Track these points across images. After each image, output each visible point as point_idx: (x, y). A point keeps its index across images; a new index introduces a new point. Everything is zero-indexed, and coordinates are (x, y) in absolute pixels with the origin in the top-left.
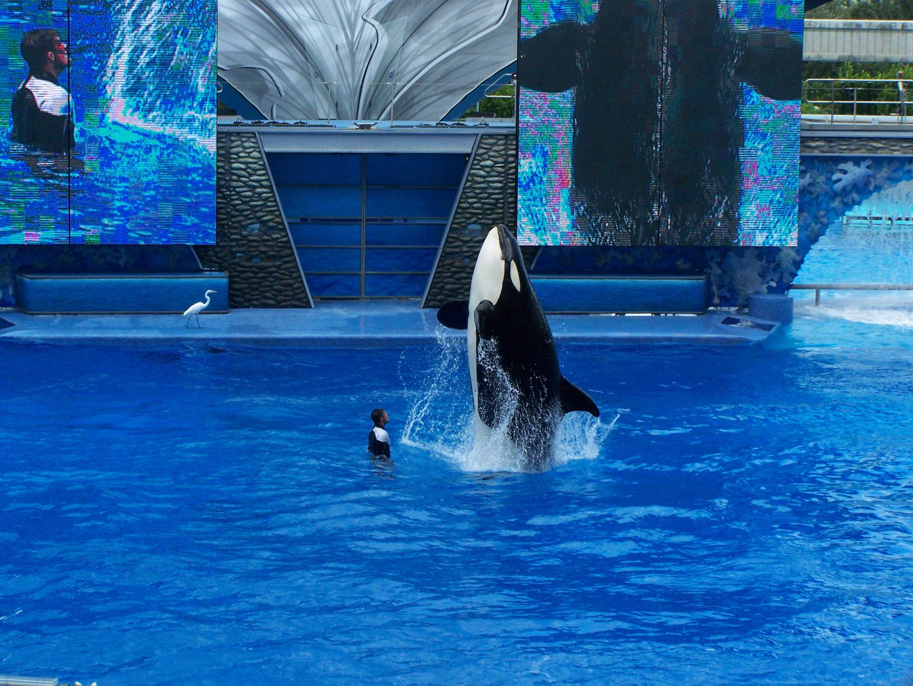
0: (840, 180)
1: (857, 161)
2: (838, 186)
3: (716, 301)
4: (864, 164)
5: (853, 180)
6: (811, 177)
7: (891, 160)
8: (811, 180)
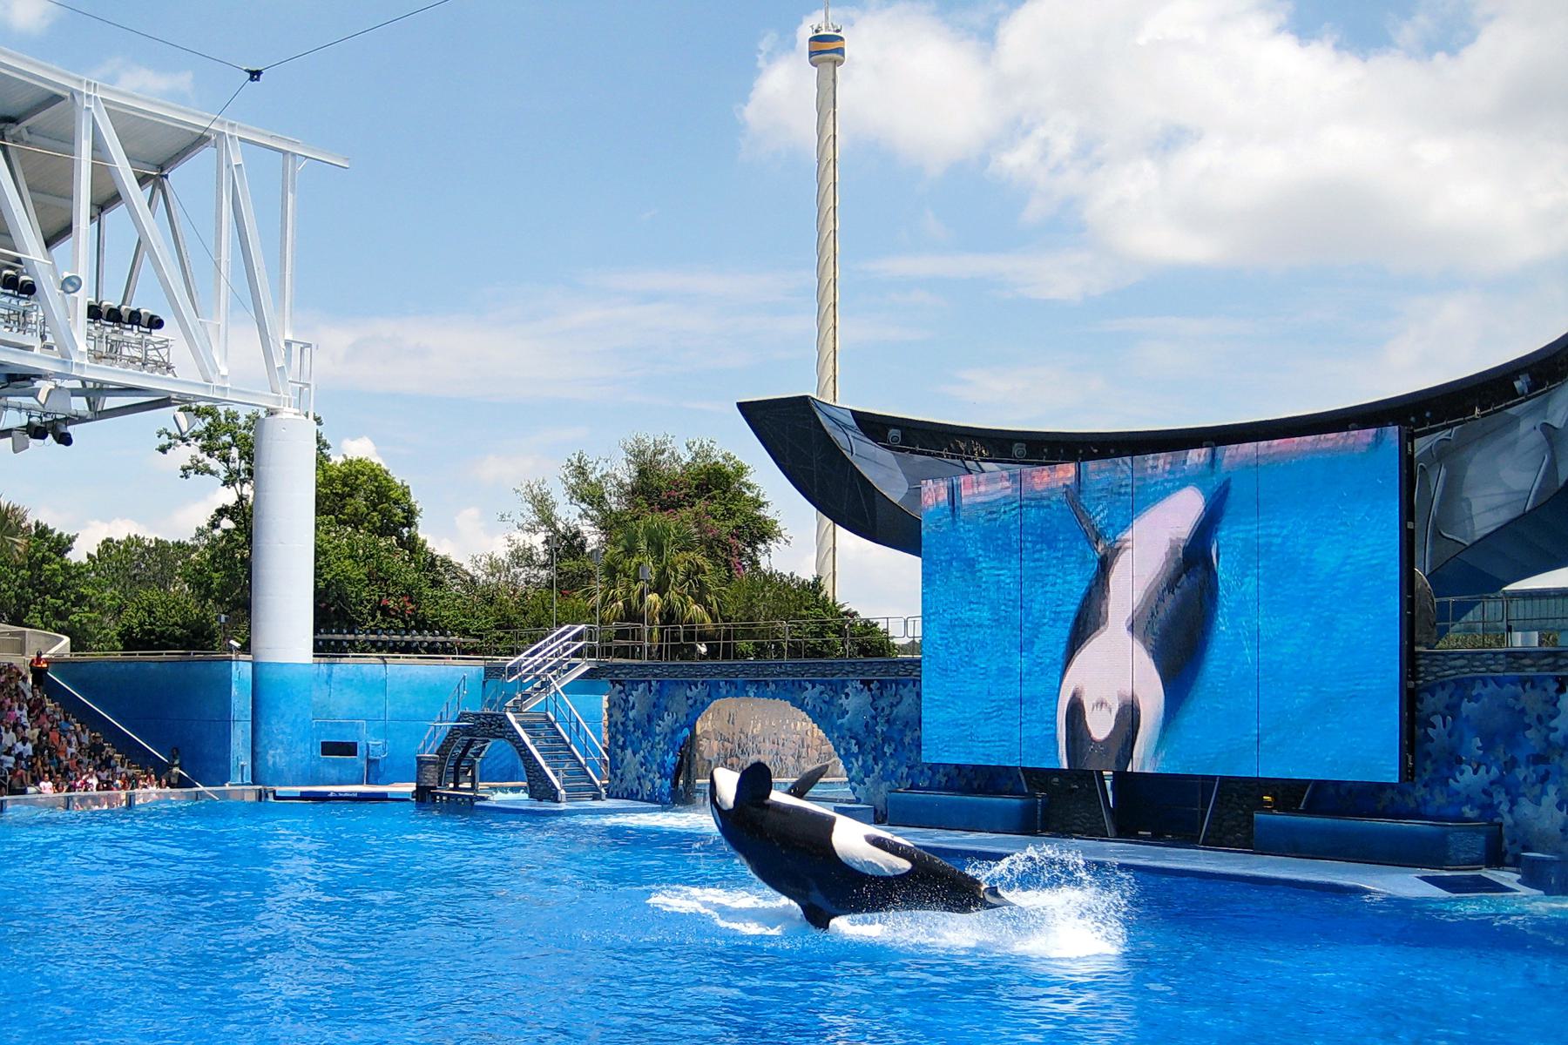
3: (1508, 859)
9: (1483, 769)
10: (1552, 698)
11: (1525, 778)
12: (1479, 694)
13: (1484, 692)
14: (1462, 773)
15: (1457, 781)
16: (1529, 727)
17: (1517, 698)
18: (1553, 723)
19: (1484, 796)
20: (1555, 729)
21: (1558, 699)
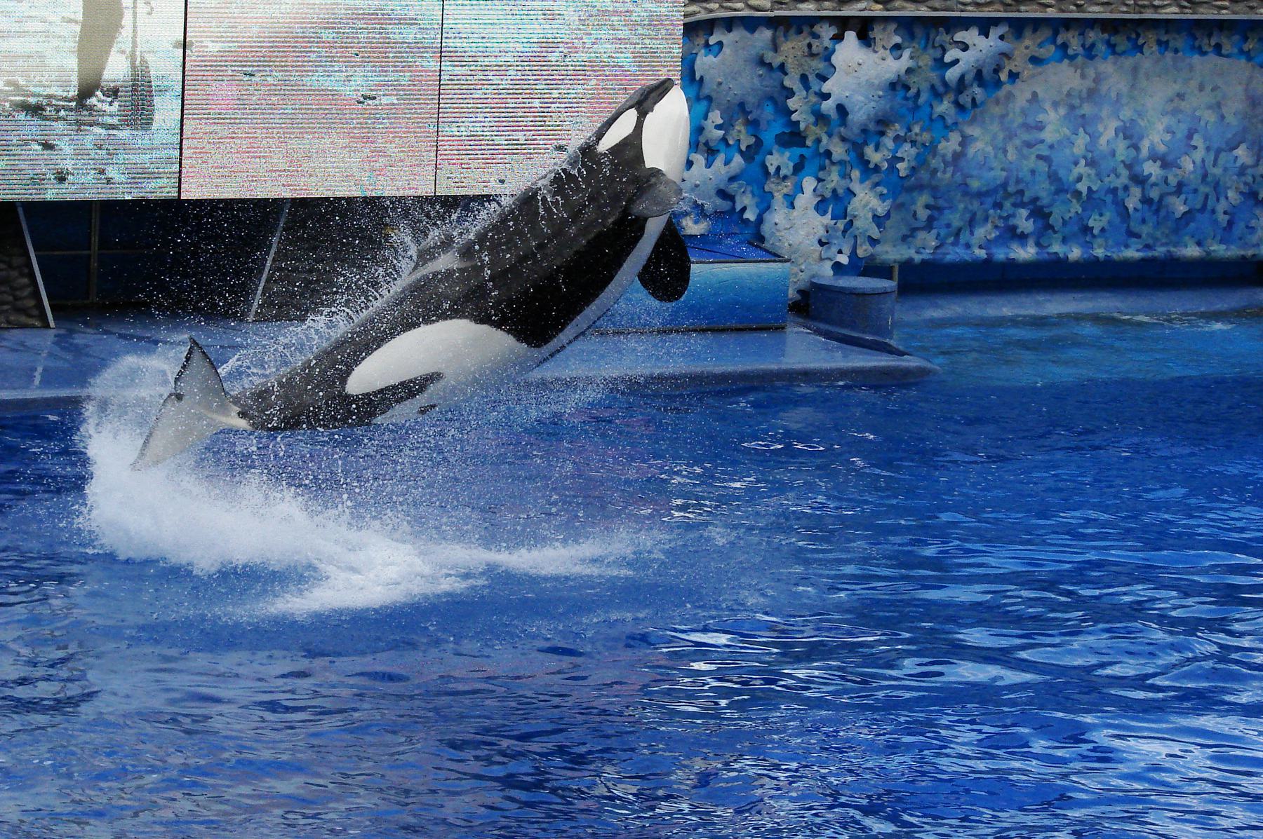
0: (956, 62)
1: (985, 26)
2: (952, 74)
4: (995, 33)
6: (912, 58)
7: (1036, 24)
8: (911, 64)
10: (826, 48)
11: (778, 169)
12: (720, 44)
13: (728, 38)
16: (790, 93)
17: (775, 48)
18: (826, 87)
19: (719, 201)
20: (826, 96)
21: (834, 51)
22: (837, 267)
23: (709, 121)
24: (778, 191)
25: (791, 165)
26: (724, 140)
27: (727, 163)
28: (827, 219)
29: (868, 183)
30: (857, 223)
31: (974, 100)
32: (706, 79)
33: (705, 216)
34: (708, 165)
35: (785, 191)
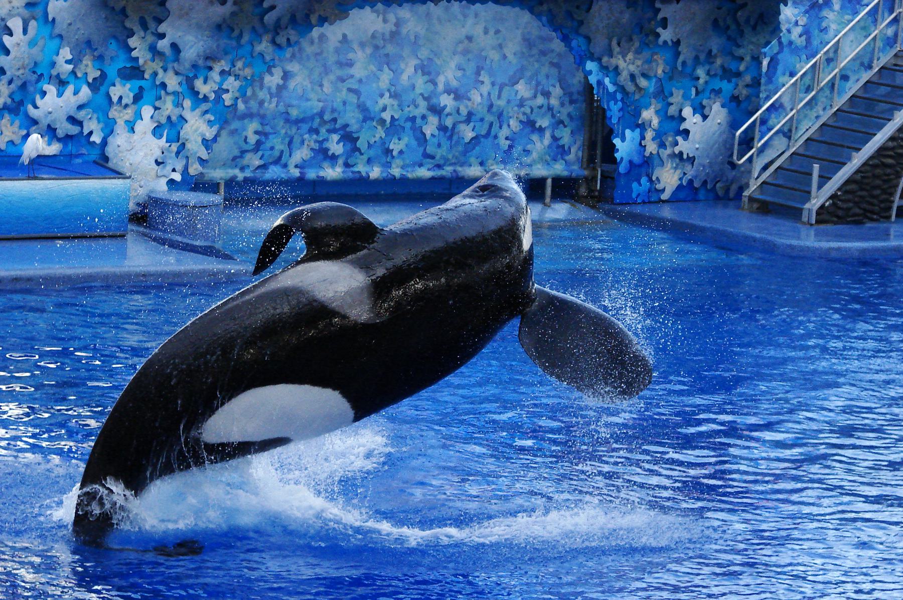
5: (291, 7)
8: (235, 8)
9: (70, 89)
11: (121, 98)
14: (44, 94)
15: (36, 107)
18: (162, 28)
20: (162, 36)
22: (171, 182)
23: (60, 56)
24: (120, 118)
25: (132, 95)
26: (73, 72)
27: (76, 93)
28: (163, 142)
29: (198, 112)
30: (188, 146)
31: (288, 40)
32: (58, 20)
33: (59, 140)
34: (60, 95)
35: (127, 117)
